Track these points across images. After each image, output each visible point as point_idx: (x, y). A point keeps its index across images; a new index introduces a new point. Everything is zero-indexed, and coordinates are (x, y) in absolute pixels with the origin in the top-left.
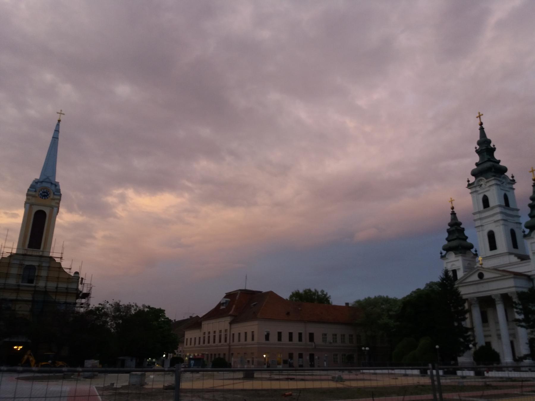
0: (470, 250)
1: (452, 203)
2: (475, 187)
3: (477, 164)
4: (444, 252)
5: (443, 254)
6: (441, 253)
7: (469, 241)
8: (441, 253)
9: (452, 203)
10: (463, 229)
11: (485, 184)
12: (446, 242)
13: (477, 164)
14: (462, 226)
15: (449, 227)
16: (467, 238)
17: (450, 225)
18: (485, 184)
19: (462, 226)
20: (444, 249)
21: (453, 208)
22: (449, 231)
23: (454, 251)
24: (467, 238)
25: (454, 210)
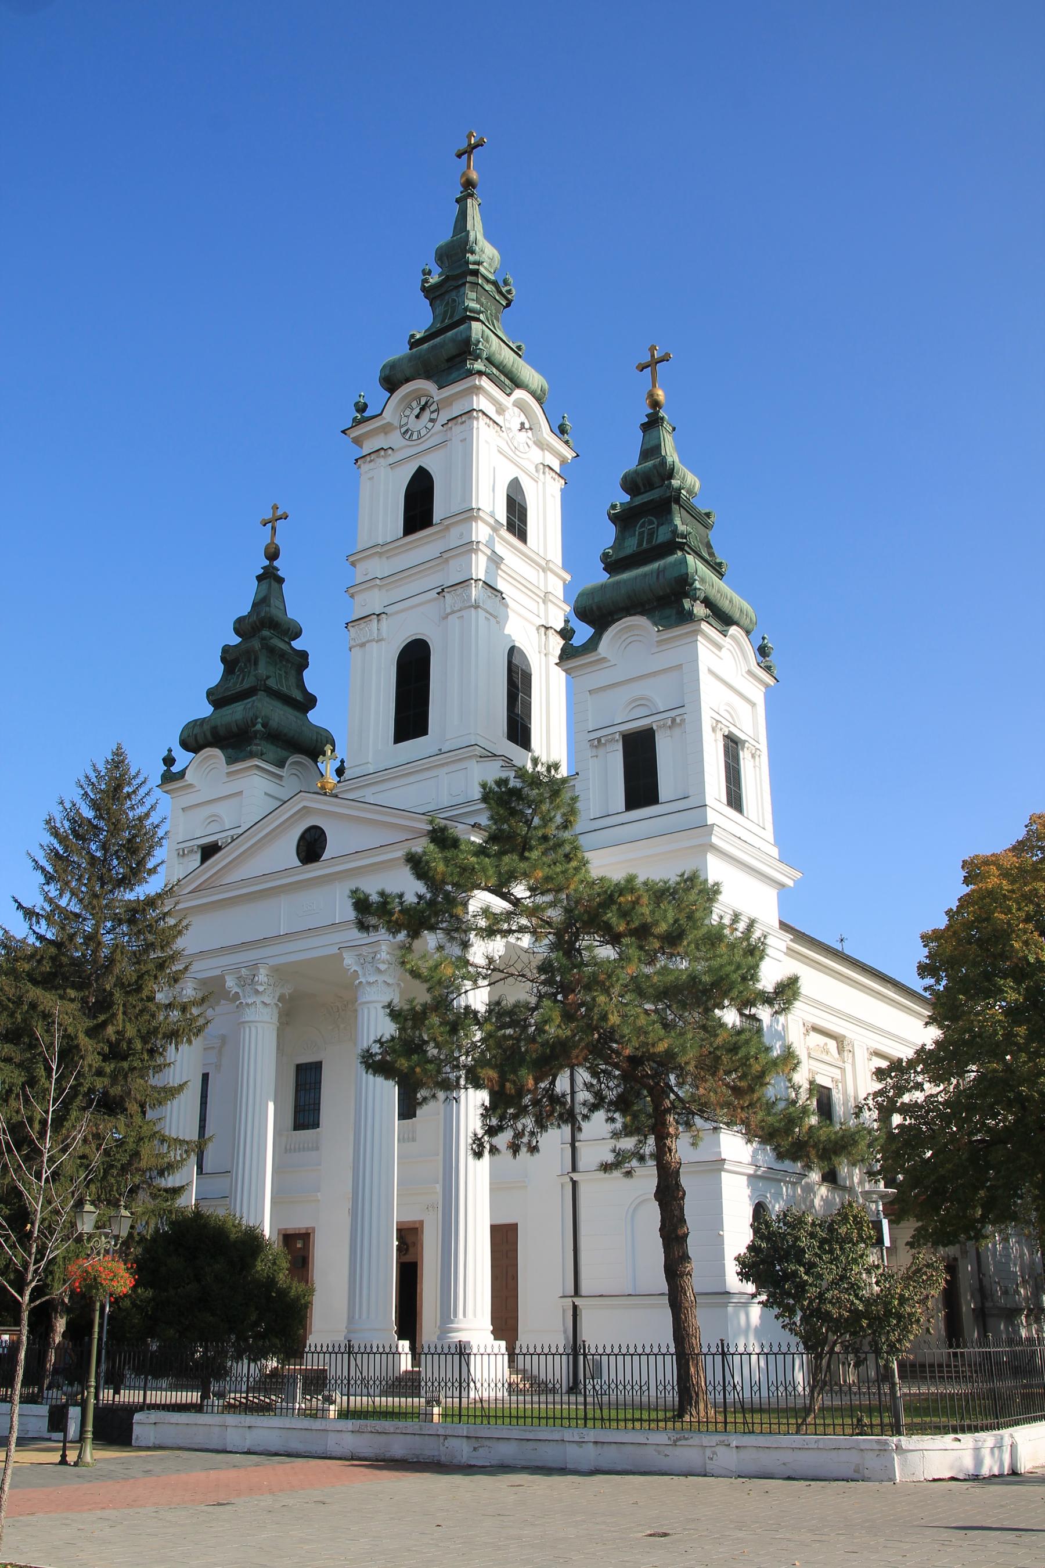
0: (316, 762)
1: (274, 529)
2: (386, 429)
3: (414, 344)
4: (183, 758)
5: (175, 769)
6: (169, 761)
7: (314, 716)
8: (169, 761)
9: (274, 529)
10: (302, 660)
11: (434, 416)
12: (206, 710)
13: (414, 344)
14: (297, 644)
15: (236, 640)
16: (311, 702)
17: (240, 625)
18: (434, 416)
19: (297, 644)
20: (185, 745)
21: (273, 554)
22: (231, 659)
23: (230, 751)
24: (311, 702)
25: (276, 563)
